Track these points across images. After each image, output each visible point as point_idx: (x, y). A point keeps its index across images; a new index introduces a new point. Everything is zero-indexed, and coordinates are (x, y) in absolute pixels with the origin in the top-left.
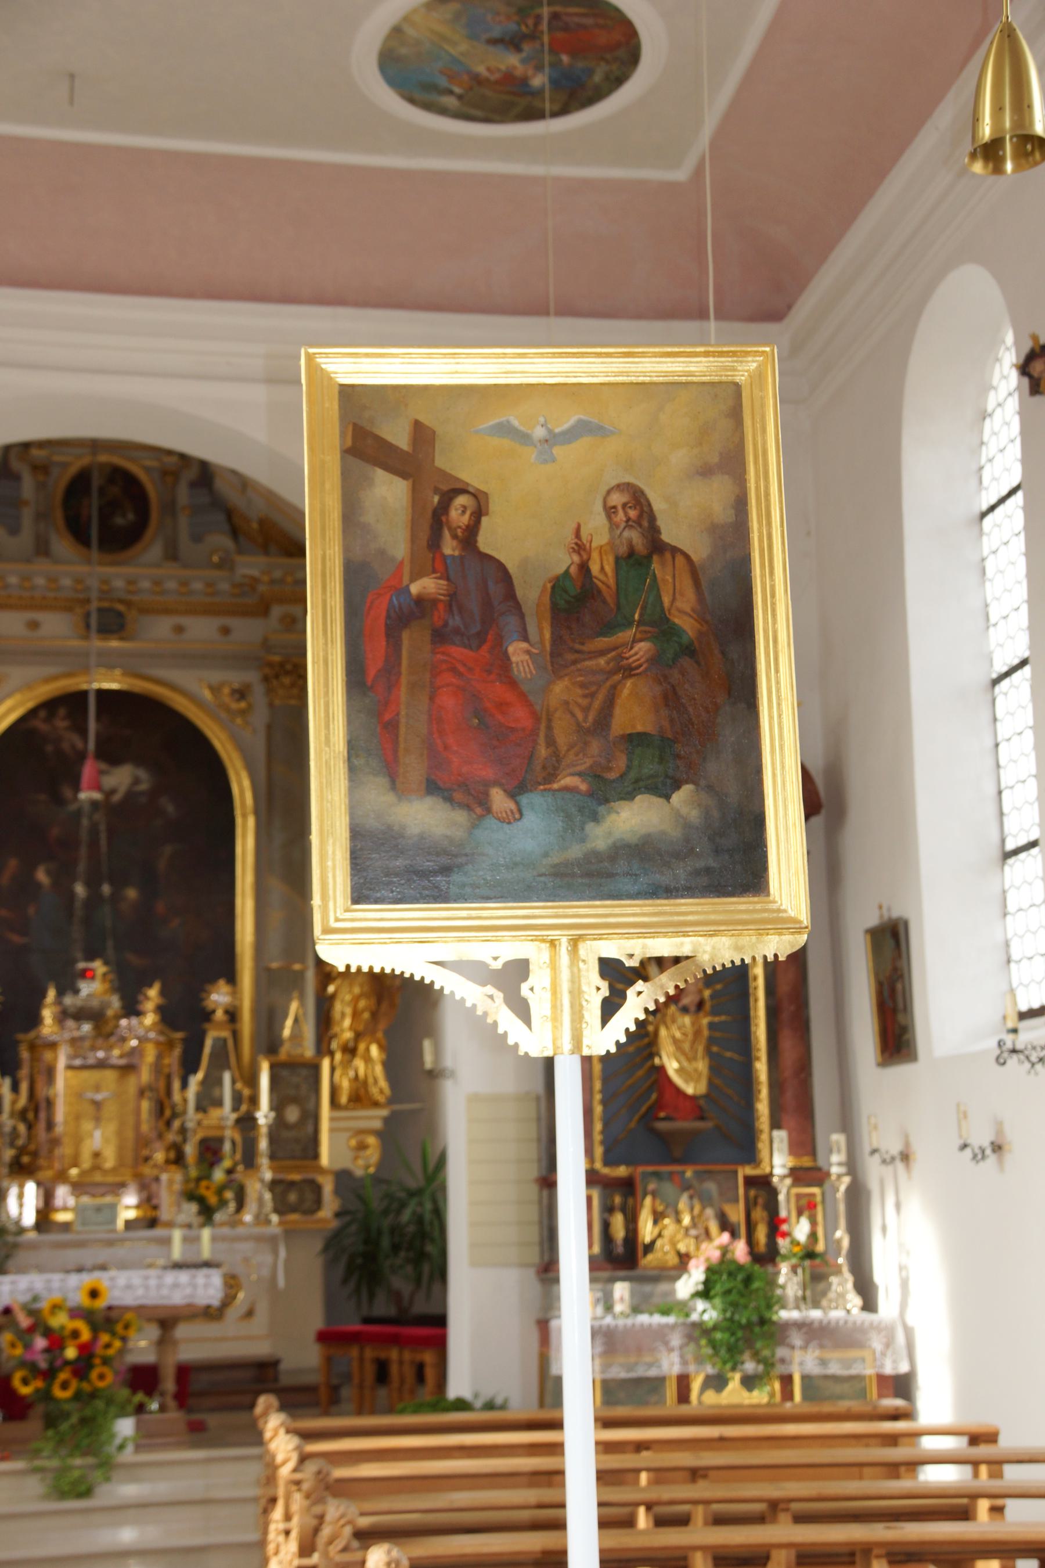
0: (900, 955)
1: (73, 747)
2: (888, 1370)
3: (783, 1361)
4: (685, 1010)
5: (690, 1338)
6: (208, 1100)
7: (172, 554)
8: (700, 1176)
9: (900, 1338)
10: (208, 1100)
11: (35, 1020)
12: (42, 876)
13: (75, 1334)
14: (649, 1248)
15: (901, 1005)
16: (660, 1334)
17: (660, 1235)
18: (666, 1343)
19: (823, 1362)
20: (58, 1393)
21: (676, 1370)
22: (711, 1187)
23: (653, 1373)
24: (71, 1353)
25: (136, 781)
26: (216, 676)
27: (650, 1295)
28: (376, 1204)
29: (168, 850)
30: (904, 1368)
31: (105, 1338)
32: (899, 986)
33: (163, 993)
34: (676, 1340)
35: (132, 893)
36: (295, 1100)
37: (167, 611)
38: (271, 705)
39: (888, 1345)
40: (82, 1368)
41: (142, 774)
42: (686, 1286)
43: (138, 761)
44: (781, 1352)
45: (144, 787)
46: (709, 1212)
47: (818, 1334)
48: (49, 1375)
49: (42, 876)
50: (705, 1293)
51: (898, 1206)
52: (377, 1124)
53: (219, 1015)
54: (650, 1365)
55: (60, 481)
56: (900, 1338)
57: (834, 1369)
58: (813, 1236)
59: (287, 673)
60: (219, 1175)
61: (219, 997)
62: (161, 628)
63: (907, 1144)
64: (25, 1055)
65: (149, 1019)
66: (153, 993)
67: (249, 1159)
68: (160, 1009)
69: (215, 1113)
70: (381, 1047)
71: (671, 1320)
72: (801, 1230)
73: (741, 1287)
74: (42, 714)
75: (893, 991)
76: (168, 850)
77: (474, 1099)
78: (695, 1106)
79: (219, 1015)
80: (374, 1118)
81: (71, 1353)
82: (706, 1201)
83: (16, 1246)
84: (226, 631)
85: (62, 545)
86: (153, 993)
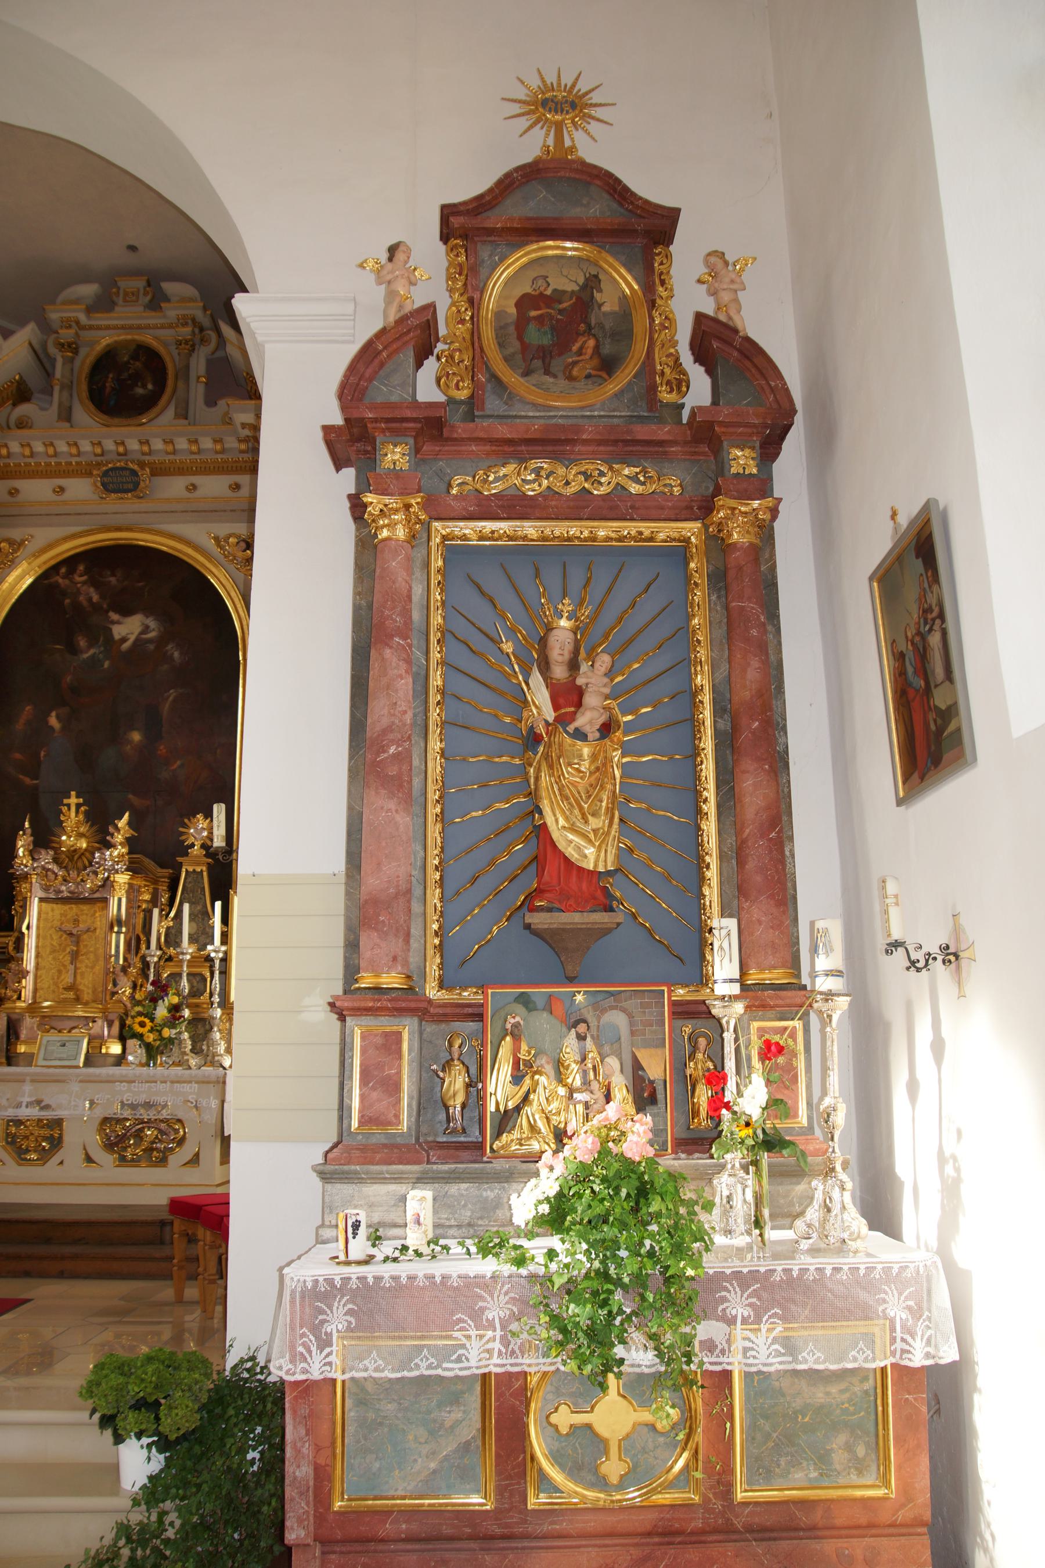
0: (936, 579)
1: (90, 599)
2: (917, 1360)
3: (710, 1346)
5: (523, 1307)
7: (183, 413)
8: (598, 1005)
9: (942, 1297)
11: (12, 854)
12: (53, 721)
14: (506, 1120)
16: (465, 1296)
17: (526, 1099)
18: (477, 1315)
19: (790, 1347)
22: (617, 1019)
23: (451, 1369)
25: (146, 629)
29: (172, 694)
30: (949, 1354)
32: (935, 639)
34: (496, 1310)
35: (136, 737)
37: (181, 470)
39: (916, 1313)
41: (152, 623)
42: (526, 1203)
43: (148, 611)
44: (706, 1330)
45: (152, 635)
46: (613, 1062)
47: (780, 1294)
49: (53, 721)
50: (556, 1217)
54: (444, 1355)
55: (87, 357)
56: (942, 1297)
57: (811, 1360)
58: (774, 1105)
62: (175, 486)
63: (957, 931)
65: (120, 850)
66: (122, 823)
68: (129, 841)
71: (488, 1266)
72: (751, 1097)
73: (627, 1211)
74: (63, 570)
75: (922, 654)
76: (172, 694)
82: (608, 1043)
85: (83, 415)
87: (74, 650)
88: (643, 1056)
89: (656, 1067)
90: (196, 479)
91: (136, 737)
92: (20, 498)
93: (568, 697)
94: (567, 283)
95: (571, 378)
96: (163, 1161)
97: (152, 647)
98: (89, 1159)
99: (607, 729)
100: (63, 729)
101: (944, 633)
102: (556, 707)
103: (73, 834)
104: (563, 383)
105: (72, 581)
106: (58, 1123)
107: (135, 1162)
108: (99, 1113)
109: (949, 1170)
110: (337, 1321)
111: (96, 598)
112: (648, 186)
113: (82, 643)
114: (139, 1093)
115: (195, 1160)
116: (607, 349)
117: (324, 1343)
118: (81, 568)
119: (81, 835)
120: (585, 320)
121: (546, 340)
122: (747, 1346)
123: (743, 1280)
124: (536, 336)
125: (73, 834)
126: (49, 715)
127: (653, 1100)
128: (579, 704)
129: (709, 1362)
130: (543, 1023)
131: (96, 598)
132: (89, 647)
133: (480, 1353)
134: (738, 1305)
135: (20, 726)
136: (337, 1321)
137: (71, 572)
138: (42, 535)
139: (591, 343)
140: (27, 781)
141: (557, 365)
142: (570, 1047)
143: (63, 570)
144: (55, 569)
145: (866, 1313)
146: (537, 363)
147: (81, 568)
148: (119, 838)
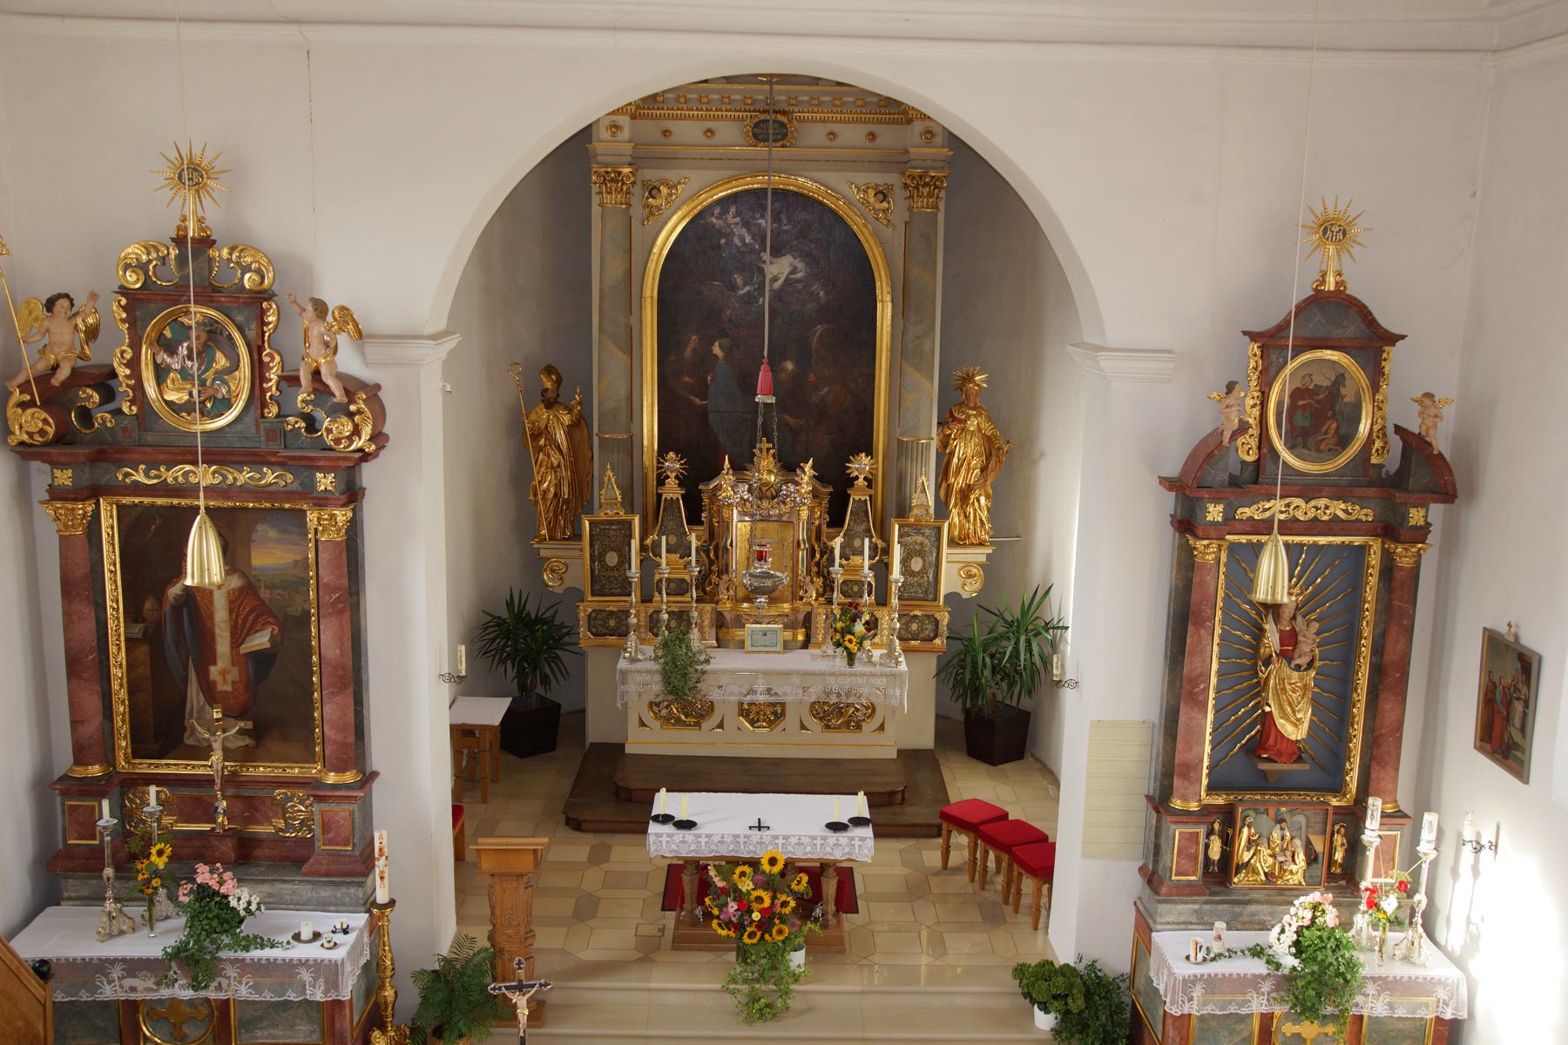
0: (1528, 683)
1: (743, 239)
4: (1298, 668)
5: (1278, 988)
6: (849, 551)
10: (849, 551)
12: (717, 350)
13: (759, 899)
15: (1517, 721)
19: (1391, 1007)
20: (746, 940)
21: (1265, 1009)
22: (1301, 819)
23: (1244, 1011)
24: (756, 916)
25: (794, 270)
26: (864, 178)
27: (1241, 914)
28: (978, 634)
31: (783, 898)
32: (1518, 706)
33: (813, 467)
35: (789, 366)
36: (921, 554)
38: (910, 209)
40: (765, 926)
41: (800, 265)
45: (799, 275)
46: (1297, 842)
48: (739, 927)
49: (717, 350)
51: (1476, 871)
52: (983, 559)
53: (861, 482)
57: (1400, 1012)
59: (926, 184)
60: (859, 628)
61: (861, 465)
64: (706, 501)
66: (808, 467)
67: (882, 601)
69: (856, 560)
70: (987, 497)
77: (1097, 724)
78: (1296, 752)
79: (861, 482)
80: (980, 555)
81: (756, 916)
83: (704, 672)
84: (872, 136)
86: (808, 467)
87: (734, 288)
88: (1313, 838)
89: (1319, 845)
90: (834, 127)
91: (789, 366)
92: (673, 139)
93: (1290, 639)
94: (1323, 380)
95: (1319, 451)
96: (859, 727)
97: (800, 286)
98: (803, 727)
99: (1310, 665)
100: (725, 357)
101: (1525, 715)
102: (1282, 644)
103: (766, 470)
104: (1314, 454)
105: (725, 221)
106: (783, 705)
107: (838, 728)
108: (813, 699)
109: (1472, 928)
110: (1197, 992)
111: (748, 240)
112: (1388, 320)
113: (739, 281)
114: (847, 682)
115: (881, 728)
116: (1343, 431)
117: (1191, 999)
118: (733, 210)
119: (770, 472)
120: (1332, 408)
121: (1306, 423)
122: (1373, 1005)
123: (1374, 979)
124: (1302, 421)
125: (766, 470)
126: (712, 344)
127: (1316, 860)
128: (1296, 644)
129: (1354, 1011)
130: (1265, 821)
131: (748, 240)
132: (746, 283)
133: (1257, 1005)
134: (1371, 989)
135: (688, 353)
136: (1197, 992)
137: (724, 212)
138: (695, 178)
139: (1334, 425)
140: (697, 401)
141: (1311, 441)
142: (1276, 835)
143: (717, 211)
144: (707, 211)
145: (1430, 994)
146: (1300, 440)
147: (733, 210)
148: (806, 478)
